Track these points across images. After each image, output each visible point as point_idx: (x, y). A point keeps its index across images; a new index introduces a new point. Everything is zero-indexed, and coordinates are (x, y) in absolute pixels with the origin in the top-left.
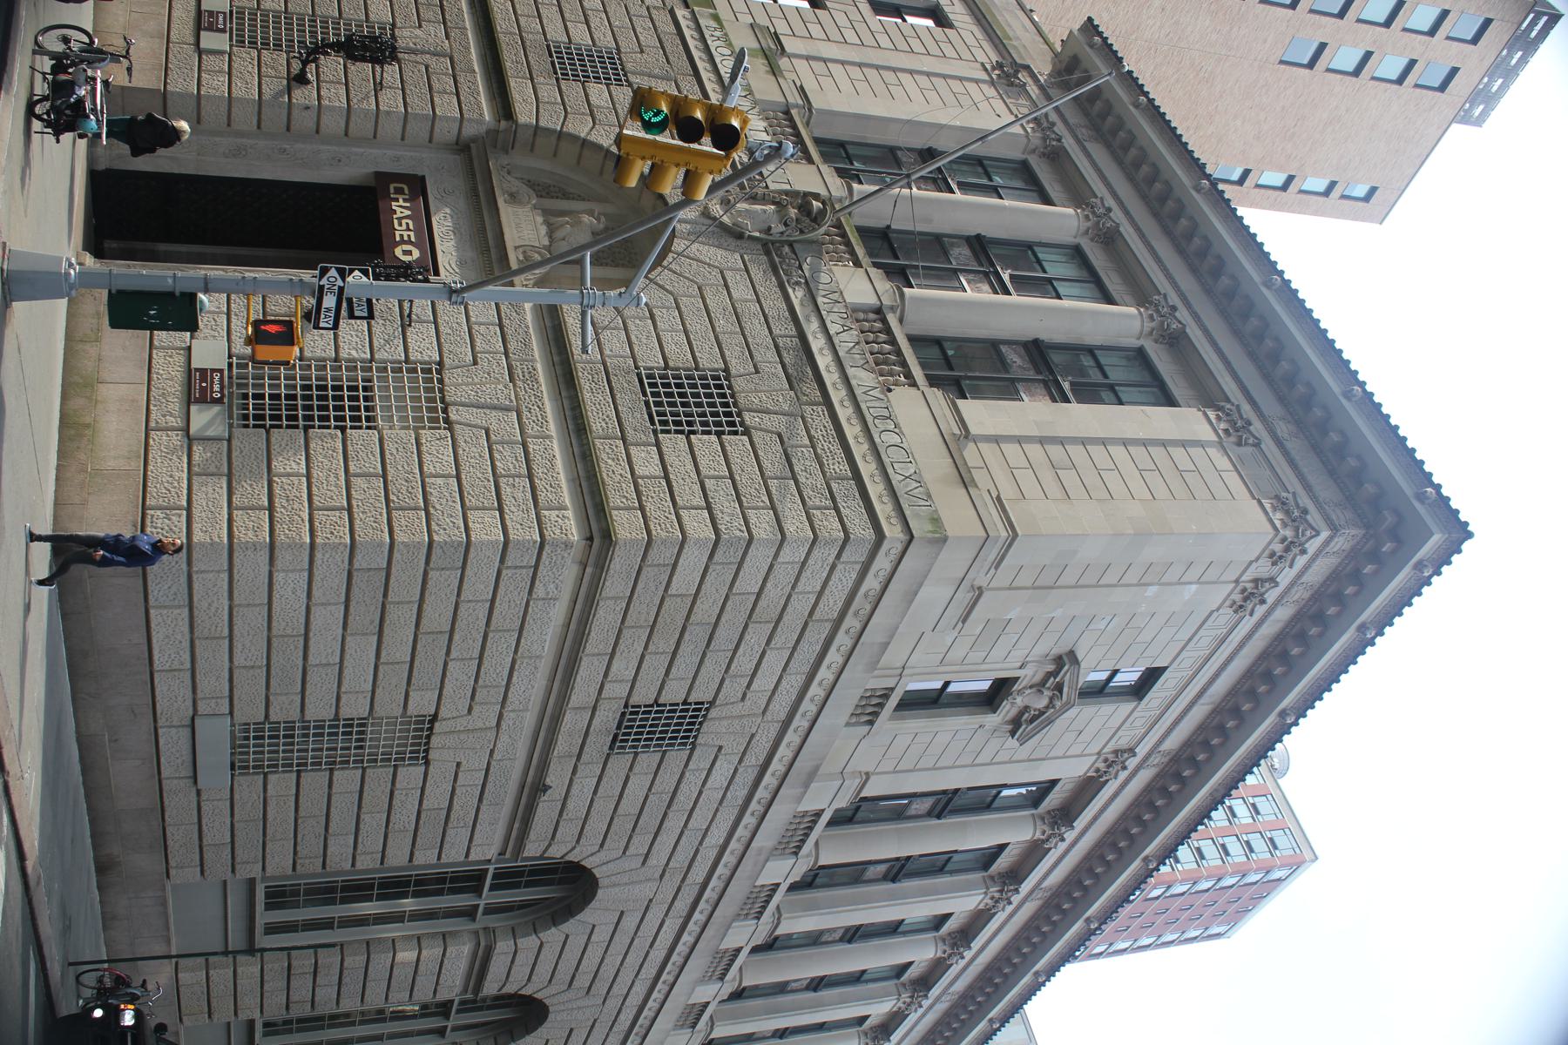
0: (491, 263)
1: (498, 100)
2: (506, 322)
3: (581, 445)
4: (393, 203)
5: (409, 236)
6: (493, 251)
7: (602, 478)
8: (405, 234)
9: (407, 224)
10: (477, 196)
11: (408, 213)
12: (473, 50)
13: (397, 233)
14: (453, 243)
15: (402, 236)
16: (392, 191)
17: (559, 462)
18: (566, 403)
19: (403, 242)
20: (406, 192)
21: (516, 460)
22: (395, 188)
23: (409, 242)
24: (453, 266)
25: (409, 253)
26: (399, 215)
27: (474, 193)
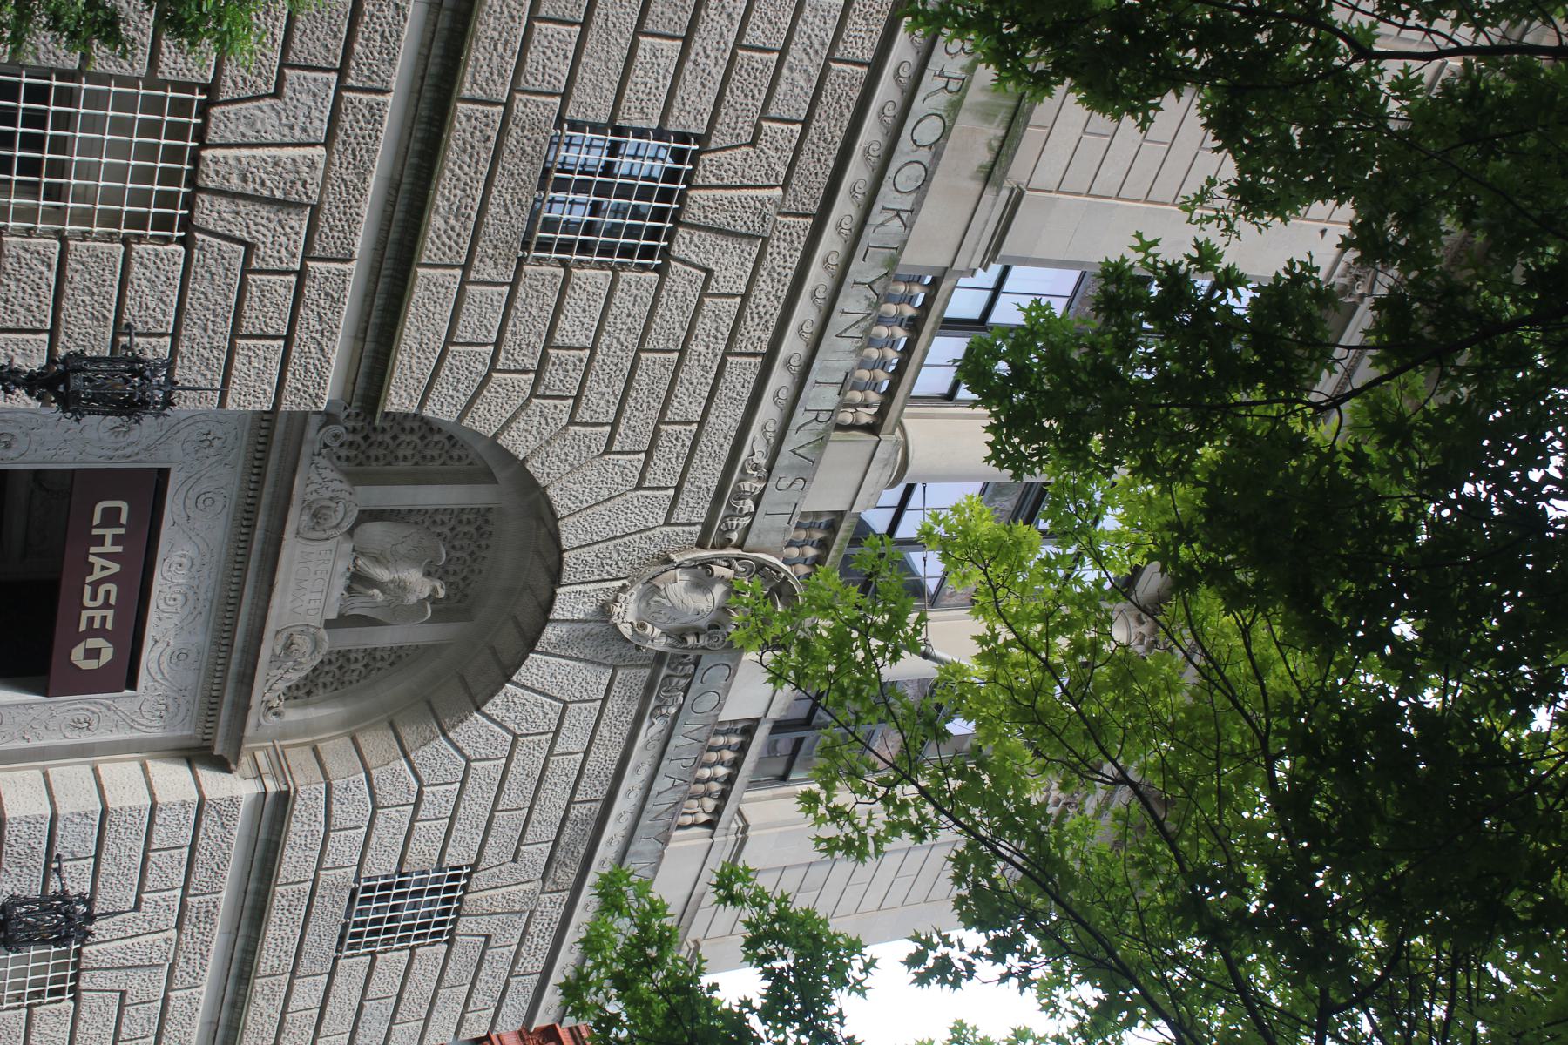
0: (225, 671)
1: (369, 346)
2: (202, 842)
3: (236, 993)
4: (93, 550)
5: (104, 618)
6: (236, 656)
7: (245, 1023)
8: (98, 614)
9: (108, 592)
10: (252, 527)
11: (115, 568)
12: (372, 180)
13: (85, 615)
14: (176, 619)
15: (91, 620)
16: (97, 520)
17: (198, 1020)
18: (240, 943)
19: (91, 632)
20: (124, 519)
21: (149, 1021)
22: (105, 510)
23: (102, 633)
24: (164, 666)
25: (93, 654)
26: (98, 574)
27: (246, 517)
